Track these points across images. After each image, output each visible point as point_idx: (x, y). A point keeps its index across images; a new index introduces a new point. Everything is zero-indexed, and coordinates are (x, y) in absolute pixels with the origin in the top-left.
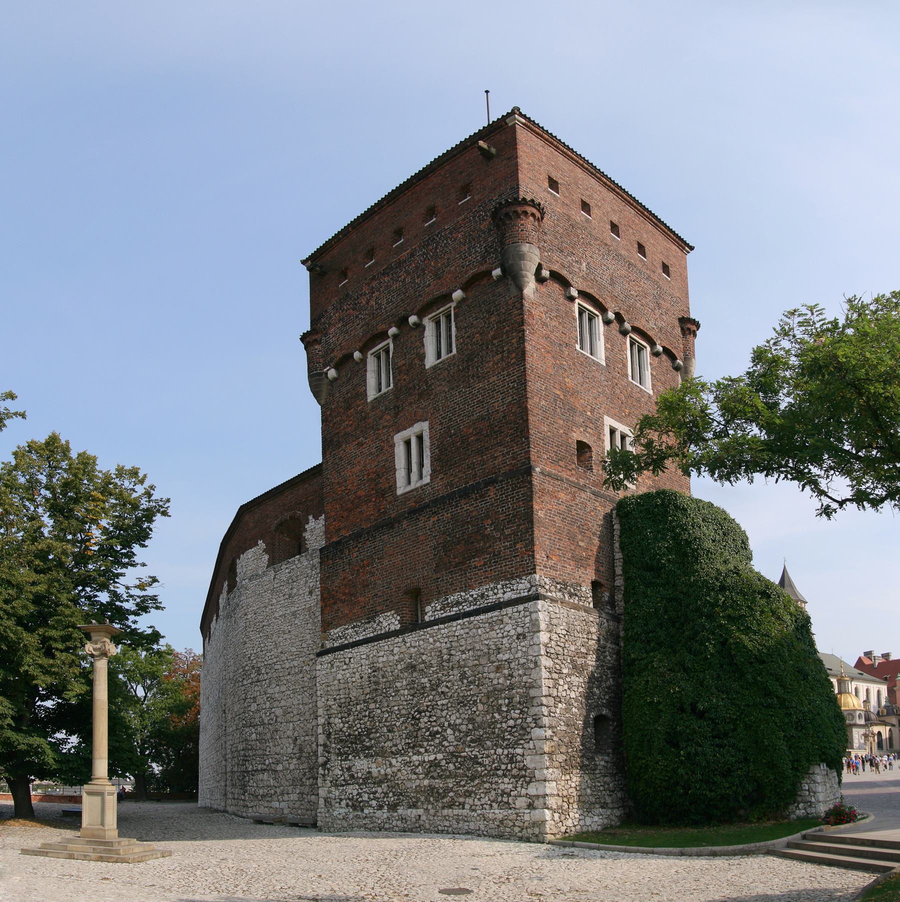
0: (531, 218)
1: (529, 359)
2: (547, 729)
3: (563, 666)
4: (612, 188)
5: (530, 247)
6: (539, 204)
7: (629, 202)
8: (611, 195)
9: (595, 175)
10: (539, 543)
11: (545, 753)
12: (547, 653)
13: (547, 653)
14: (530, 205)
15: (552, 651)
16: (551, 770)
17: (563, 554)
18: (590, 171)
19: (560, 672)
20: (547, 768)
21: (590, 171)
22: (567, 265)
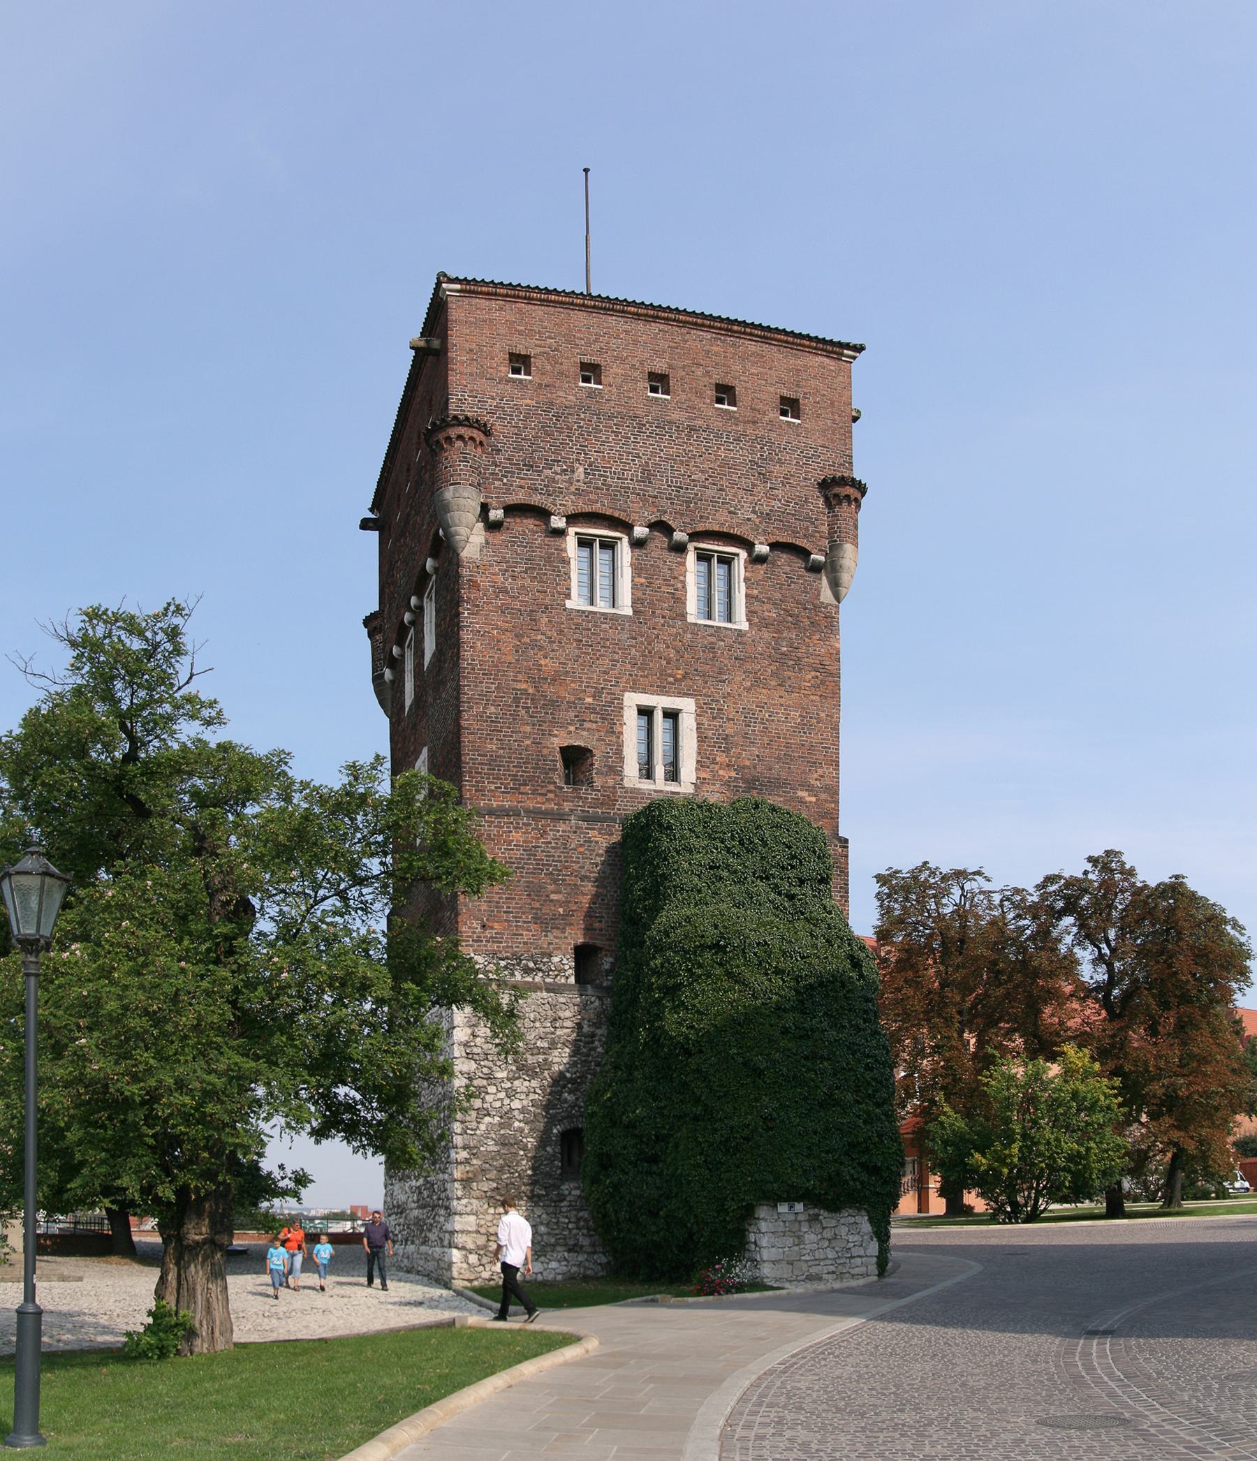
0: (459, 444)
1: (467, 654)
2: (459, 1150)
3: (494, 1068)
4: (652, 316)
5: (455, 490)
6: (467, 418)
7: (696, 324)
8: (654, 327)
9: (612, 310)
10: (468, 910)
11: (456, 1180)
12: (468, 1054)
13: (468, 1054)
14: (453, 425)
15: (476, 1050)
16: (464, 1201)
17: (513, 917)
18: (601, 308)
19: (490, 1078)
20: (459, 1199)
21: (601, 308)
22: (540, 484)
